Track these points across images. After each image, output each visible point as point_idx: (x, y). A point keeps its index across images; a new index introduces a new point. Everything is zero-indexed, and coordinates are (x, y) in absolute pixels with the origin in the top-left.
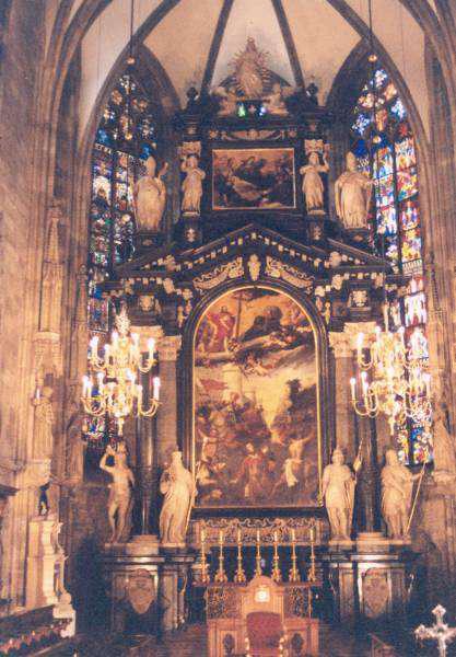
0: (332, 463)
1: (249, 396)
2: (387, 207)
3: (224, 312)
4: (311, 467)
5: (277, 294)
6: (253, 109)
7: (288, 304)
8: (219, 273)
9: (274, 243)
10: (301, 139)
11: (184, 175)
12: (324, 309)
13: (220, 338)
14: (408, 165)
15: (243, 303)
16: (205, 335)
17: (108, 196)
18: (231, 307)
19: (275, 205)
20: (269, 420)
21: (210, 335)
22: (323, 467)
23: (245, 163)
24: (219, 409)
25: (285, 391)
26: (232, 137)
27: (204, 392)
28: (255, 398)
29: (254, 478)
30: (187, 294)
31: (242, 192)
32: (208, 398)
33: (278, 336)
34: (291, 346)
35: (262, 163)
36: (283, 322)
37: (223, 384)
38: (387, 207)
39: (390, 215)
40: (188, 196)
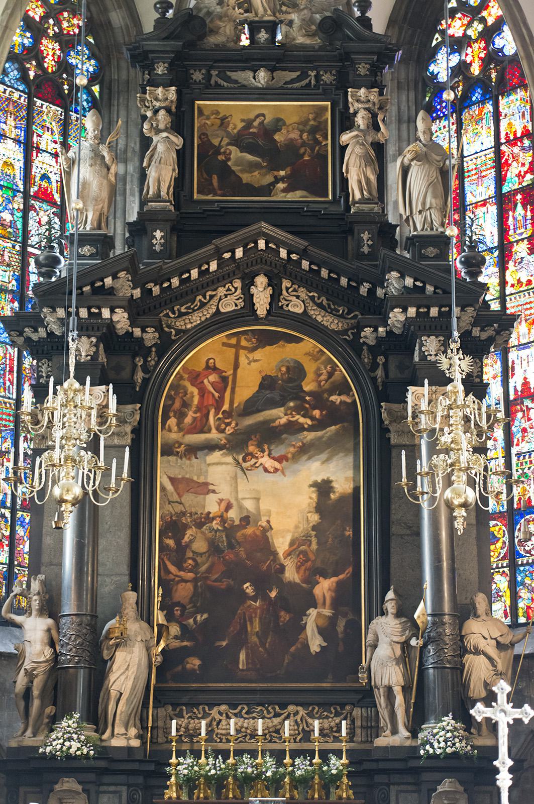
0: (383, 614)
1: (249, 505)
2: (484, 203)
3: (211, 368)
4: (346, 627)
5: (302, 340)
6: (263, 36)
7: (316, 356)
8: (203, 305)
9: (294, 257)
10: (344, 83)
11: (146, 143)
12: (374, 366)
13: (203, 411)
14: (519, 135)
15: (242, 353)
16: (177, 404)
17: (18, 173)
18: (223, 362)
19: (297, 196)
20: (281, 544)
21: (186, 405)
22: (370, 619)
23: (249, 124)
24: (199, 525)
25: (307, 498)
26: (228, 79)
27: (175, 497)
28: (258, 508)
29: (255, 639)
30: (151, 337)
31: (242, 171)
32: (178, 508)
33: (298, 409)
34: (319, 425)
35: (278, 123)
36: (308, 386)
37: (206, 484)
40: (152, 174)
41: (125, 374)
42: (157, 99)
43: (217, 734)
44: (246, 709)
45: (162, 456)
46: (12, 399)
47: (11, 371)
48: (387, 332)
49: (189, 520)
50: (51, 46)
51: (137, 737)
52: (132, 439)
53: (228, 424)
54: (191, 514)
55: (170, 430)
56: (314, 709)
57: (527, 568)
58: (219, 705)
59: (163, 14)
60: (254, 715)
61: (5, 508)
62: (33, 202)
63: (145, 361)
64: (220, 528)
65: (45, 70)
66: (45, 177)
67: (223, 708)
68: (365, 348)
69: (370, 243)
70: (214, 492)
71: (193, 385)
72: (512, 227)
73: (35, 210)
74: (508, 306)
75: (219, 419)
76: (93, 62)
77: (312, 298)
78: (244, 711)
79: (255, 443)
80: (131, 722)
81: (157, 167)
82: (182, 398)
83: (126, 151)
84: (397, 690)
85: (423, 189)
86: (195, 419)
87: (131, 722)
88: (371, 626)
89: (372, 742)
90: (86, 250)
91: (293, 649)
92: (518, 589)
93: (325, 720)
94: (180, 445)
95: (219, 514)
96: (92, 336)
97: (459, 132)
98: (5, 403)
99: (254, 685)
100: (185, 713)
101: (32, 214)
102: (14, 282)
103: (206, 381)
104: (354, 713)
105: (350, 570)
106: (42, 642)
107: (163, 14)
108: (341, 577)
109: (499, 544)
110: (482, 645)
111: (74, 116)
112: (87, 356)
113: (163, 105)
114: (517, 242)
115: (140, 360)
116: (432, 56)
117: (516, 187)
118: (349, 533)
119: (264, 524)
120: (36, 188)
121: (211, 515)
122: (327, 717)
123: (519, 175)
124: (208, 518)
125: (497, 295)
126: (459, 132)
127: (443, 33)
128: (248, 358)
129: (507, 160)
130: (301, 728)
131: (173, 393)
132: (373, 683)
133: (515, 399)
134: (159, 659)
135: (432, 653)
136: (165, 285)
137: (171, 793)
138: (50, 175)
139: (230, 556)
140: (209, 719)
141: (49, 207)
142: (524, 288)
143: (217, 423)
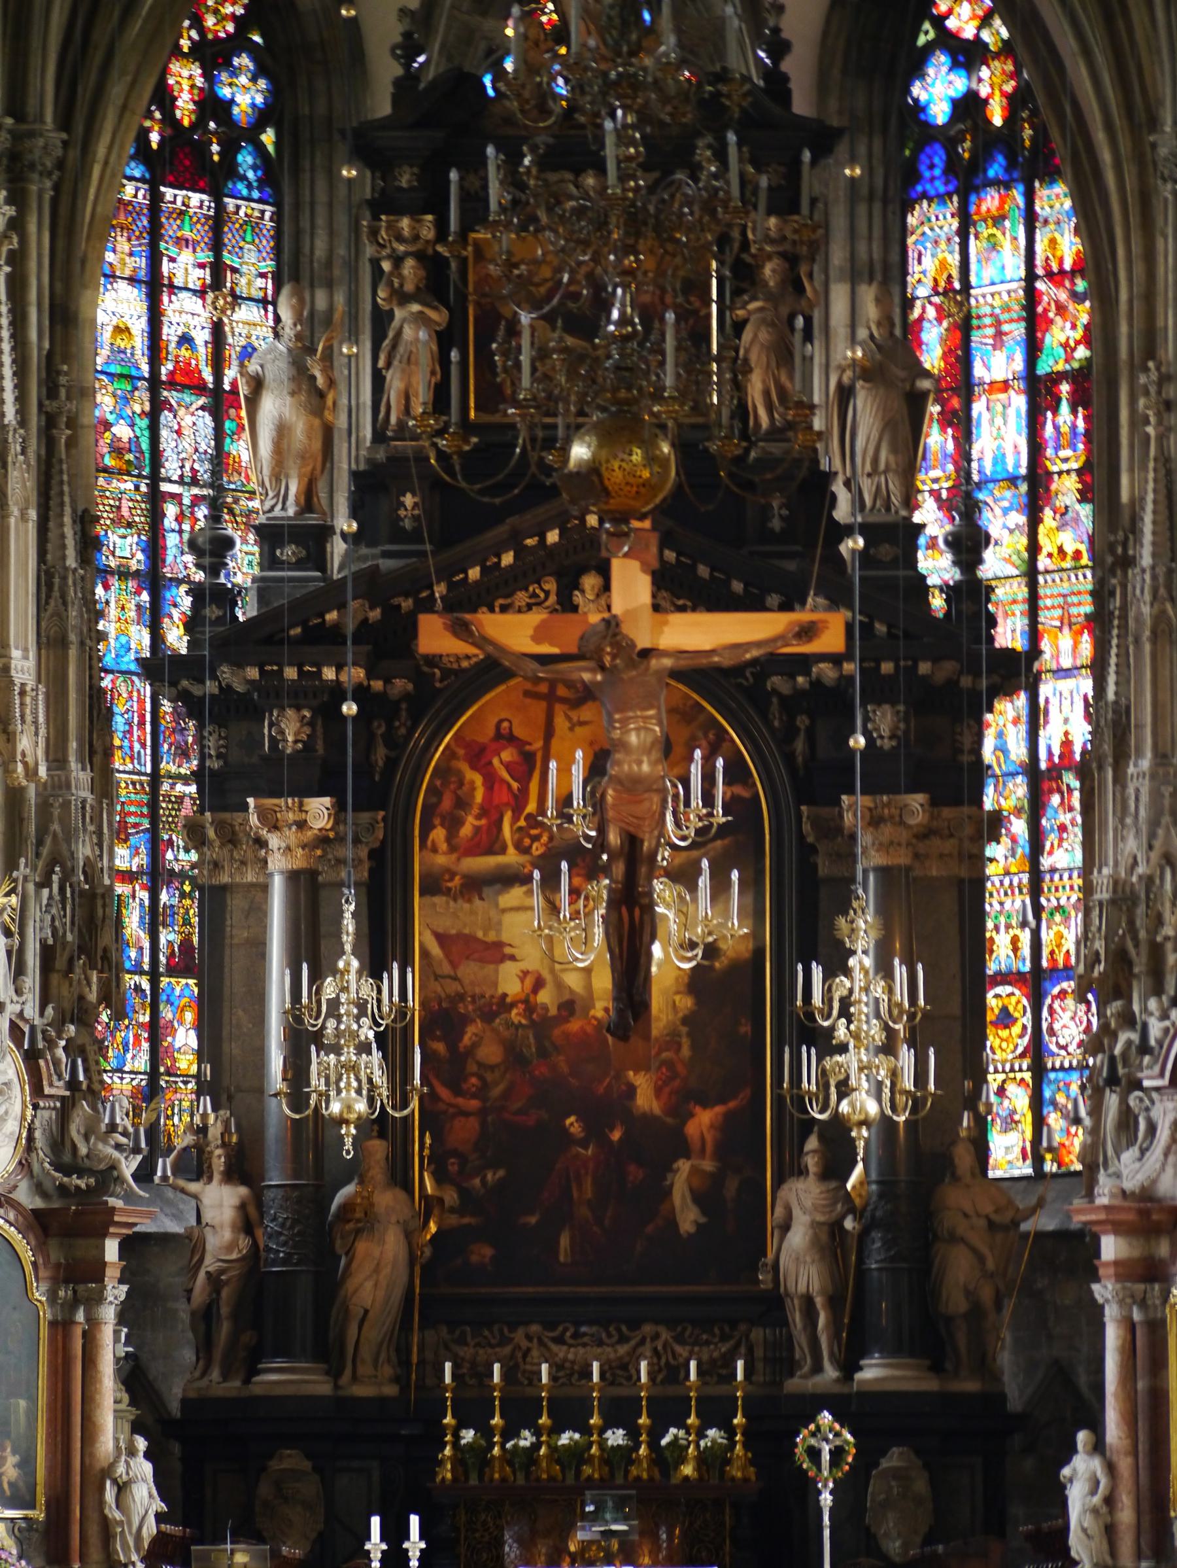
0: (802, 1172)
1: (573, 981)
2: (1005, 386)
3: (505, 738)
11: (381, 320)
12: (790, 732)
14: (1067, 266)
15: (559, 709)
16: (447, 803)
17: (139, 342)
21: (462, 803)
27: (446, 969)
28: (589, 986)
29: (584, 1212)
32: (453, 988)
37: (499, 945)
39: (1011, 412)
42: (400, 238)
43: (524, 1371)
44: (572, 1330)
45: (421, 895)
46: (145, 774)
47: (142, 723)
48: (811, 683)
49: (470, 1008)
50: (185, 73)
51: (396, 1379)
52: (371, 871)
53: (536, 838)
54: (473, 997)
55: (435, 850)
56: (685, 1329)
57: (1061, 1075)
58: (527, 1323)
59: (407, 66)
60: (586, 1339)
61: (142, 973)
62: (165, 393)
63: (390, 727)
64: (524, 1022)
65: (174, 123)
66: (186, 340)
67: (535, 1328)
68: (775, 700)
69: (785, 512)
70: (513, 958)
71: (474, 767)
72: (1051, 444)
73: (171, 409)
74: (1041, 592)
75: (521, 828)
76: (262, 84)
78: (568, 1334)
79: (583, 872)
80: (383, 1356)
81: (403, 371)
82: (455, 792)
83: (329, 264)
84: (819, 1301)
85: (875, 435)
86: (477, 829)
87: (383, 1356)
88: (783, 1193)
89: (781, 1384)
90: (288, 552)
91: (649, 1229)
92: (1045, 1112)
93: (705, 1349)
94: (453, 875)
95: (523, 996)
96: (304, 707)
98: (134, 783)
99: (584, 1289)
100: (469, 1339)
101: (166, 417)
102: (140, 556)
103: (496, 761)
104: (753, 1336)
105: (746, 1093)
106: (234, 1228)
107: (407, 66)
108: (732, 1104)
109: (1016, 1029)
110: (962, 1228)
111: (230, 203)
112: (296, 742)
113: (411, 249)
114: (1060, 473)
115: (379, 726)
116: (916, 66)
117: (1061, 367)
118: (745, 1029)
120: (170, 366)
121: (508, 1000)
122: (707, 1343)
123: (1065, 345)
124: (504, 1004)
125: (1024, 568)
126: (963, 233)
127: (939, 22)
128: (569, 718)
129: (1046, 311)
130: (663, 1361)
131: (438, 783)
132: (782, 1289)
133: (1049, 769)
134: (428, 1252)
135: (878, 1245)
136: (424, 594)
138: (193, 333)
140: (507, 1350)
141: (193, 398)
142: (1068, 564)
143: (517, 836)
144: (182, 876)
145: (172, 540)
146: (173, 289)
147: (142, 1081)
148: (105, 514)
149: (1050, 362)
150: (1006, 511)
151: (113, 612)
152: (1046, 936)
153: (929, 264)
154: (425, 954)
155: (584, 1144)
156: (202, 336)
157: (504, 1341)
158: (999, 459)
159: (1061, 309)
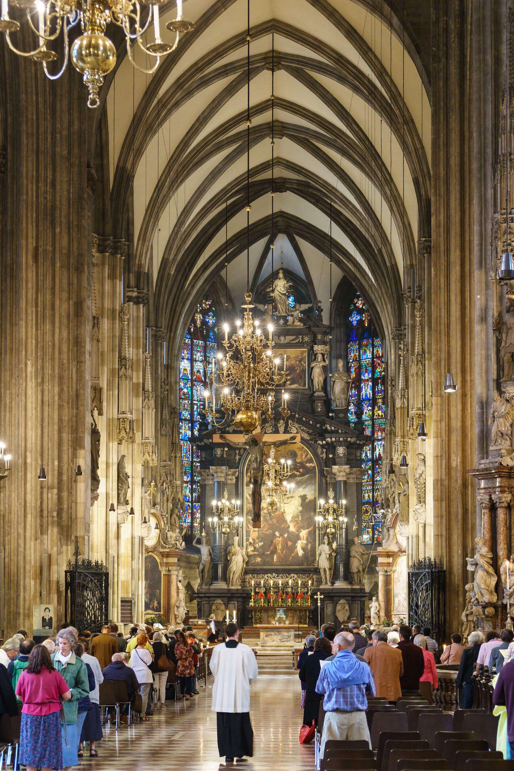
0: (324, 543)
2: (367, 380)
17: (189, 372)
20: (288, 518)
22: (319, 545)
34: (302, 475)
38: (367, 380)
41: (232, 457)
66: (198, 371)
67: (269, 575)
77: (300, 427)
84: (327, 570)
97: (359, 349)
110: (356, 555)
116: (350, 314)
119: (282, 510)
126: (359, 349)
137: (252, 604)
139: (271, 522)
144: (198, 482)
145: (196, 413)
146: (196, 361)
147: (189, 524)
148: (182, 408)
149: (377, 375)
150: (368, 407)
151: (183, 428)
152: (375, 495)
153: (352, 355)
154: (247, 498)
155: (279, 537)
156: (202, 371)
157: (263, 577)
158: (366, 395)
159: (379, 364)
